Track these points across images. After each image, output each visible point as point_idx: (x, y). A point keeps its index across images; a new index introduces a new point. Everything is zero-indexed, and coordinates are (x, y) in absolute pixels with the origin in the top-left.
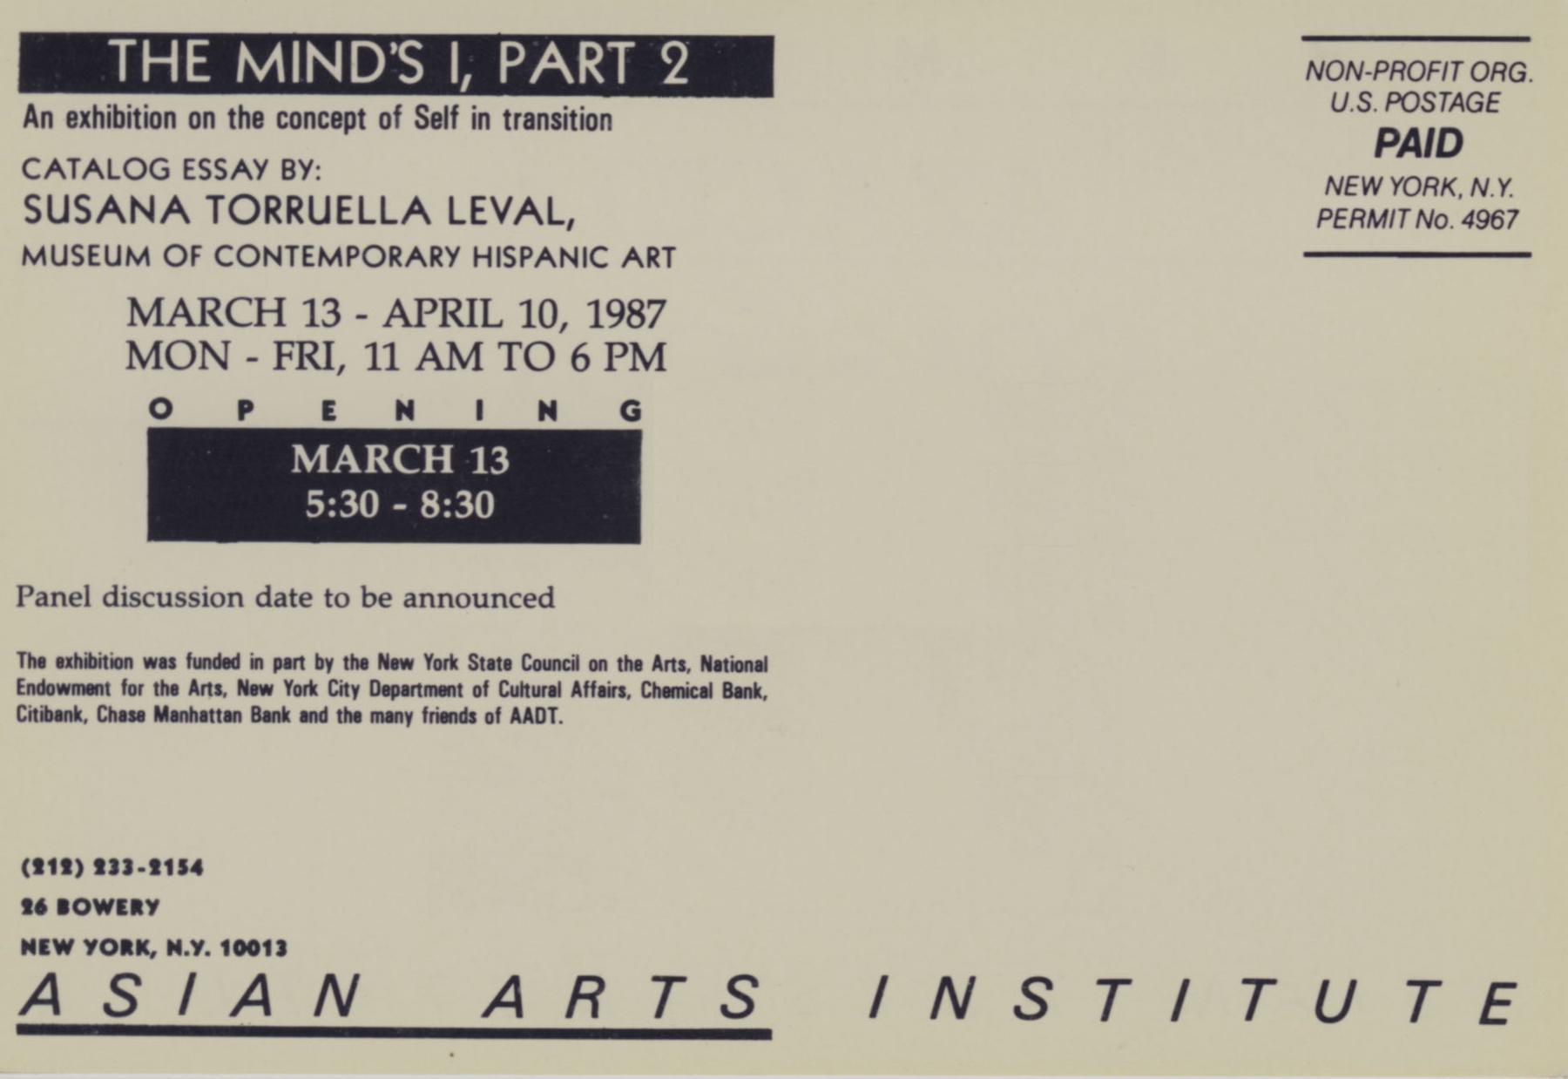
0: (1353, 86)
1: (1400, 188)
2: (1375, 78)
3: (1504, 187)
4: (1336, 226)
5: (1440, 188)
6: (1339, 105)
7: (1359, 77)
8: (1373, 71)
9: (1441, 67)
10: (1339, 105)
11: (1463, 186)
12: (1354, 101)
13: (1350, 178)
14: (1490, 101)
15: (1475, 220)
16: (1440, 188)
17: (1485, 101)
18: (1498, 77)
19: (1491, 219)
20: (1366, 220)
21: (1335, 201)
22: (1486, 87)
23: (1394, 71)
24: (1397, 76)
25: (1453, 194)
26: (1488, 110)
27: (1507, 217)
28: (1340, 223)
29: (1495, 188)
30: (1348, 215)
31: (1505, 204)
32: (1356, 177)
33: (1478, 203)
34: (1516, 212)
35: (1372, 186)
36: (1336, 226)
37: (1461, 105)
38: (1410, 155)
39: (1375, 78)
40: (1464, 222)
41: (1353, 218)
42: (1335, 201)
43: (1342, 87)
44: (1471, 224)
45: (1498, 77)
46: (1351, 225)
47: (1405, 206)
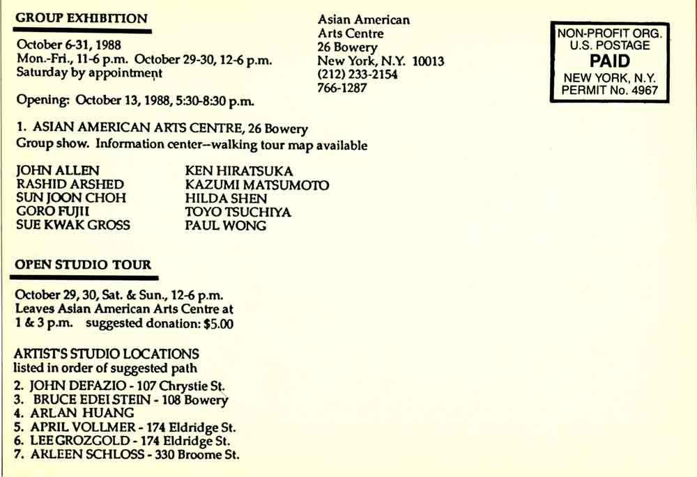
0: (580, 40)
1: (601, 79)
2: (588, 36)
3: (650, 78)
4: (571, 93)
5: (619, 78)
6: (574, 46)
7: (582, 36)
8: (587, 33)
9: (619, 31)
10: (574, 46)
11: (630, 77)
12: (580, 45)
13: (574, 74)
14: (644, 45)
15: (638, 90)
16: (619, 78)
17: (642, 44)
18: (646, 36)
19: (646, 90)
20: (586, 90)
21: (568, 83)
22: (641, 39)
23: (597, 33)
24: (599, 35)
25: (626, 81)
26: (644, 49)
27: (653, 89)
28: (573, 92)
29: (645, 78)
30: (577, 88)
31: (652, 84)
32: (579, 74)
33: (638, 84)
34: (657, 87)
35: (587, 77)
36: (571, 93)
37: (631, 46)
38: (606, 66)
39: (588, 36)
40: (633, 91)
41: (579, 90)
42: (568, 83)
43: (574, 39)
44: (636, 92)
45: (646, 36)
46: (579, 93)
47: (603, 85)
